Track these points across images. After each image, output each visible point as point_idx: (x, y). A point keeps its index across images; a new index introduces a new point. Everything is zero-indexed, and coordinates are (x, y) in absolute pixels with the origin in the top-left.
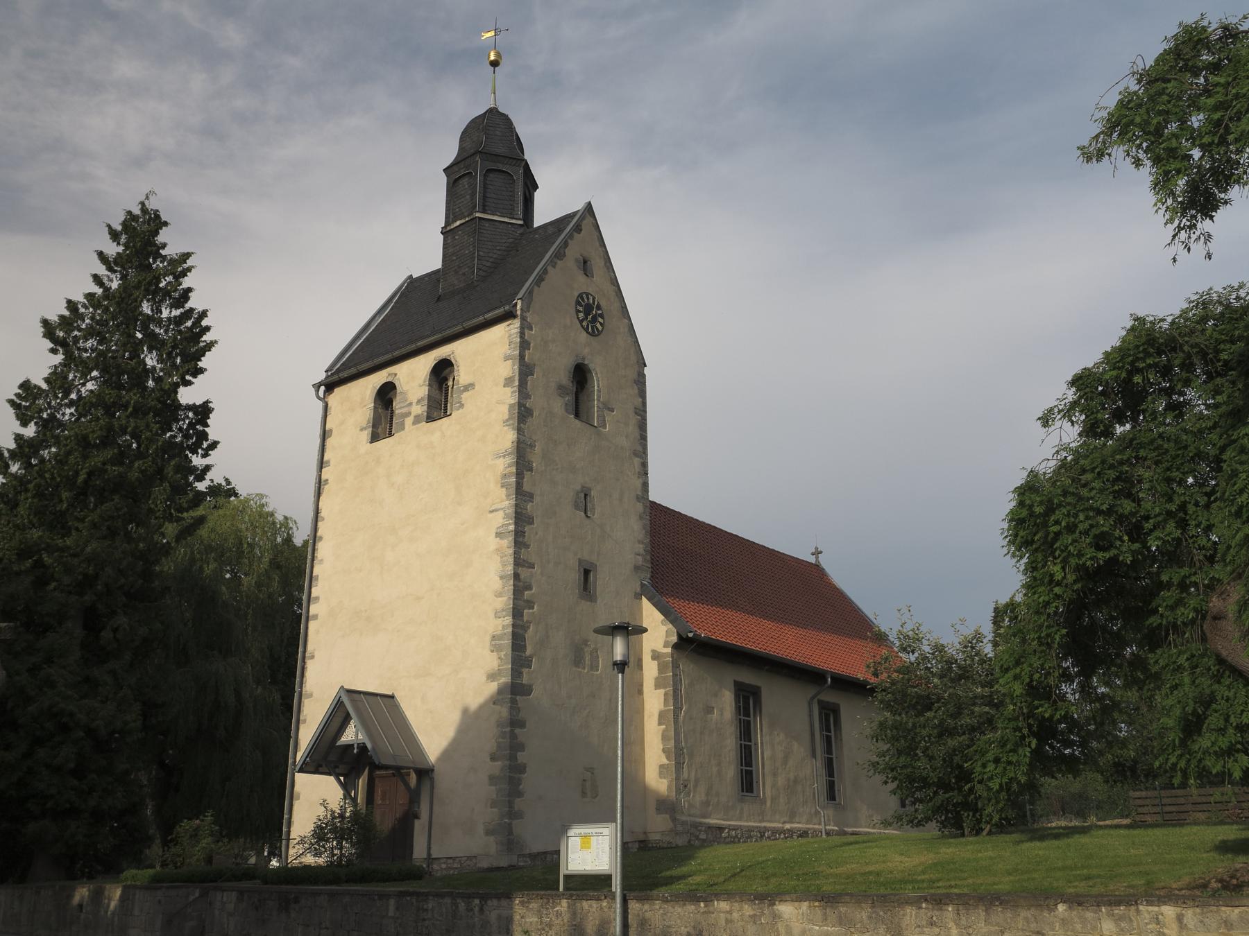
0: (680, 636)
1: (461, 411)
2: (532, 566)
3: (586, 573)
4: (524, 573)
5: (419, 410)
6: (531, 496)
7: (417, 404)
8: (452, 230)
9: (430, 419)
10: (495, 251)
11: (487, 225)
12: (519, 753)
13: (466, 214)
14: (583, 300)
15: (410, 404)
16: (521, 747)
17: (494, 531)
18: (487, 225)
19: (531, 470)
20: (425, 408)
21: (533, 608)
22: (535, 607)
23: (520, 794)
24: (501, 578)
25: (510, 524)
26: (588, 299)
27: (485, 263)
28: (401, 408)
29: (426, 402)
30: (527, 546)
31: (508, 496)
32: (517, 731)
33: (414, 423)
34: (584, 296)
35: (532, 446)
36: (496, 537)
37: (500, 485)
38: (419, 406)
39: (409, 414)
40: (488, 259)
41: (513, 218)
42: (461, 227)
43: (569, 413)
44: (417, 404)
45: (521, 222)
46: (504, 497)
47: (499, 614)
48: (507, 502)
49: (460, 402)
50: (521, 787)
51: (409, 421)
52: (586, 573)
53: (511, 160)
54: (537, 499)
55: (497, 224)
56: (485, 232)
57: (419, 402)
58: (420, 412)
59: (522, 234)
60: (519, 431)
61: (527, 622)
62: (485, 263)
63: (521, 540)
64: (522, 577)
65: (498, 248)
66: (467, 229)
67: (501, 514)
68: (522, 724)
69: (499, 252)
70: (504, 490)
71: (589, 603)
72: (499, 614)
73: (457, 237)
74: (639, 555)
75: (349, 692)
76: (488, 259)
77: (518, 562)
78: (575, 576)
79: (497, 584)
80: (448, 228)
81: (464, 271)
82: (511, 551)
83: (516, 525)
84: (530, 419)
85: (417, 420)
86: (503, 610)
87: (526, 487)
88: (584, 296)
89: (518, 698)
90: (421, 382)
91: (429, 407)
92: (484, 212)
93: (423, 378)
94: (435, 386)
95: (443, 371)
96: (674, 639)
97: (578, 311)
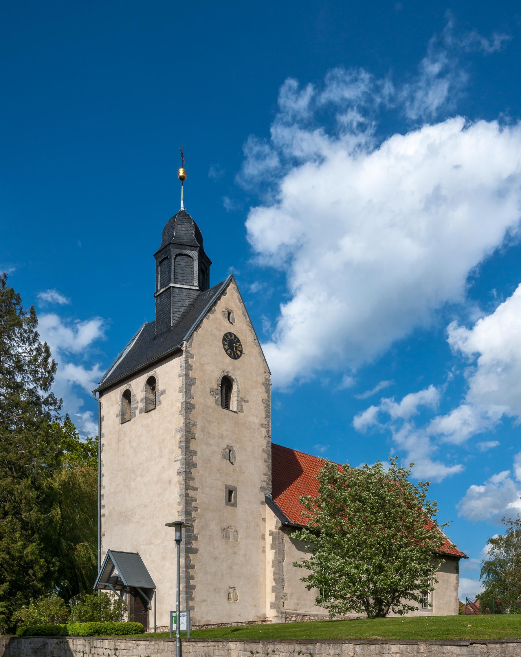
0: (282, 524)
1: (160, 406)
2: (196, 489)
3: (230, 492)
4: (191, 493)
5: (141, 405)
6: (195, 453)
7: (140, 402)
8: (159, 295)
9: (147, 411)
10: (183, 308)
11: (177, 291)
12: (191, 581)
13: (166, 284)
14: (228, 337)
15: (137, 402)
16: (193, 578)
17: (176, 471)
18: (177, 291)
19: (194, 438)
20: (144, 404)
21: (197, 511)
22: (199, 510)
23: (193, 599)
24: (180, 496)
25: (183, 468)
26: (231, 336)
27: (176, 315)
28: (133, 404)
29: (144, 401)
30: (193, 479)
31: (182, 453)
32: (190, 570)
33: (140, 413)
34: (228, 335)
35: (195, 425)
36: (177, 475)
37: (178, 447)
38: (142, 403)
39: (136, 408)
40: (178, 313)
41: (193, 286)
42: (164, 293)
43: (218, 405)
44: (140, 402)
45: (197, 288)
46: (180, 453)
47: (180, 514)
48: (182, 456)
49: (159, 401)
50: (193, 596)
51: (137, 411)
52: (230, 492)
53: (193, 248)
54: (199, 454)
55: (183, 290)
56: (176, 295)
57: (141, 400)
58: (142, 406)
59: (198, 296)
60: (187, 418)
61: (194, 517)
62: (176, 315)
63: (189, 476)
64: (190, 495)
65: (184, 305)
66: (167, 294)
67: (179, 463)
68: (193, 567)
69: (185, 308)
70: (180, 450)
71: (232, 508)
72: (180, 514)
73: (162, 299)
74: (264, 481)
75: (112, 551)
76: (178, 313)
77: (188, 487)
78: (222, 495)
79: (178, 499)
80: (158, 294)
81: (166, 321)
82: (183, 482)
83: (186, 468)
84: (193, 411)
85: (140, 412)
86: (181, 512)
87: (192, 447)
88: (228, 335)
89: (189, 554)
90: (142, 389)
91: (146, 404)
92: (175, 283)
93: (142, 387)
94: (150, 391)
95: (152, 382)
96: (280, 525)
97: (224, 345)
